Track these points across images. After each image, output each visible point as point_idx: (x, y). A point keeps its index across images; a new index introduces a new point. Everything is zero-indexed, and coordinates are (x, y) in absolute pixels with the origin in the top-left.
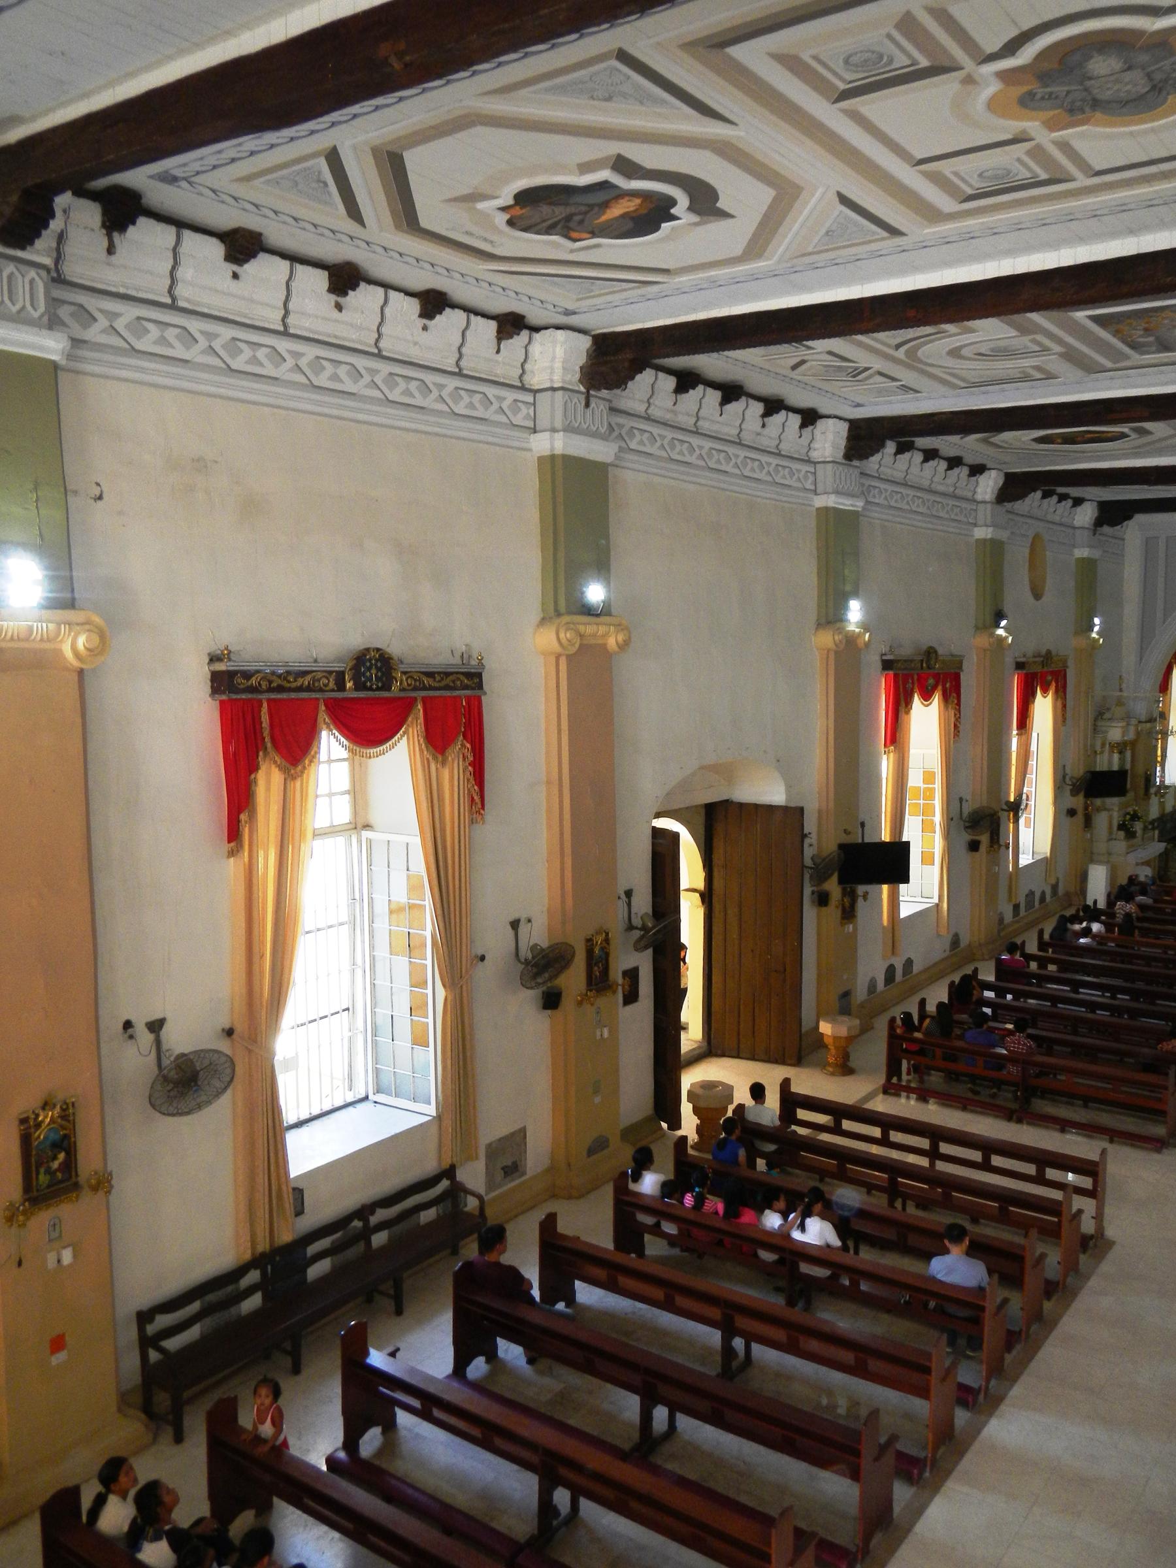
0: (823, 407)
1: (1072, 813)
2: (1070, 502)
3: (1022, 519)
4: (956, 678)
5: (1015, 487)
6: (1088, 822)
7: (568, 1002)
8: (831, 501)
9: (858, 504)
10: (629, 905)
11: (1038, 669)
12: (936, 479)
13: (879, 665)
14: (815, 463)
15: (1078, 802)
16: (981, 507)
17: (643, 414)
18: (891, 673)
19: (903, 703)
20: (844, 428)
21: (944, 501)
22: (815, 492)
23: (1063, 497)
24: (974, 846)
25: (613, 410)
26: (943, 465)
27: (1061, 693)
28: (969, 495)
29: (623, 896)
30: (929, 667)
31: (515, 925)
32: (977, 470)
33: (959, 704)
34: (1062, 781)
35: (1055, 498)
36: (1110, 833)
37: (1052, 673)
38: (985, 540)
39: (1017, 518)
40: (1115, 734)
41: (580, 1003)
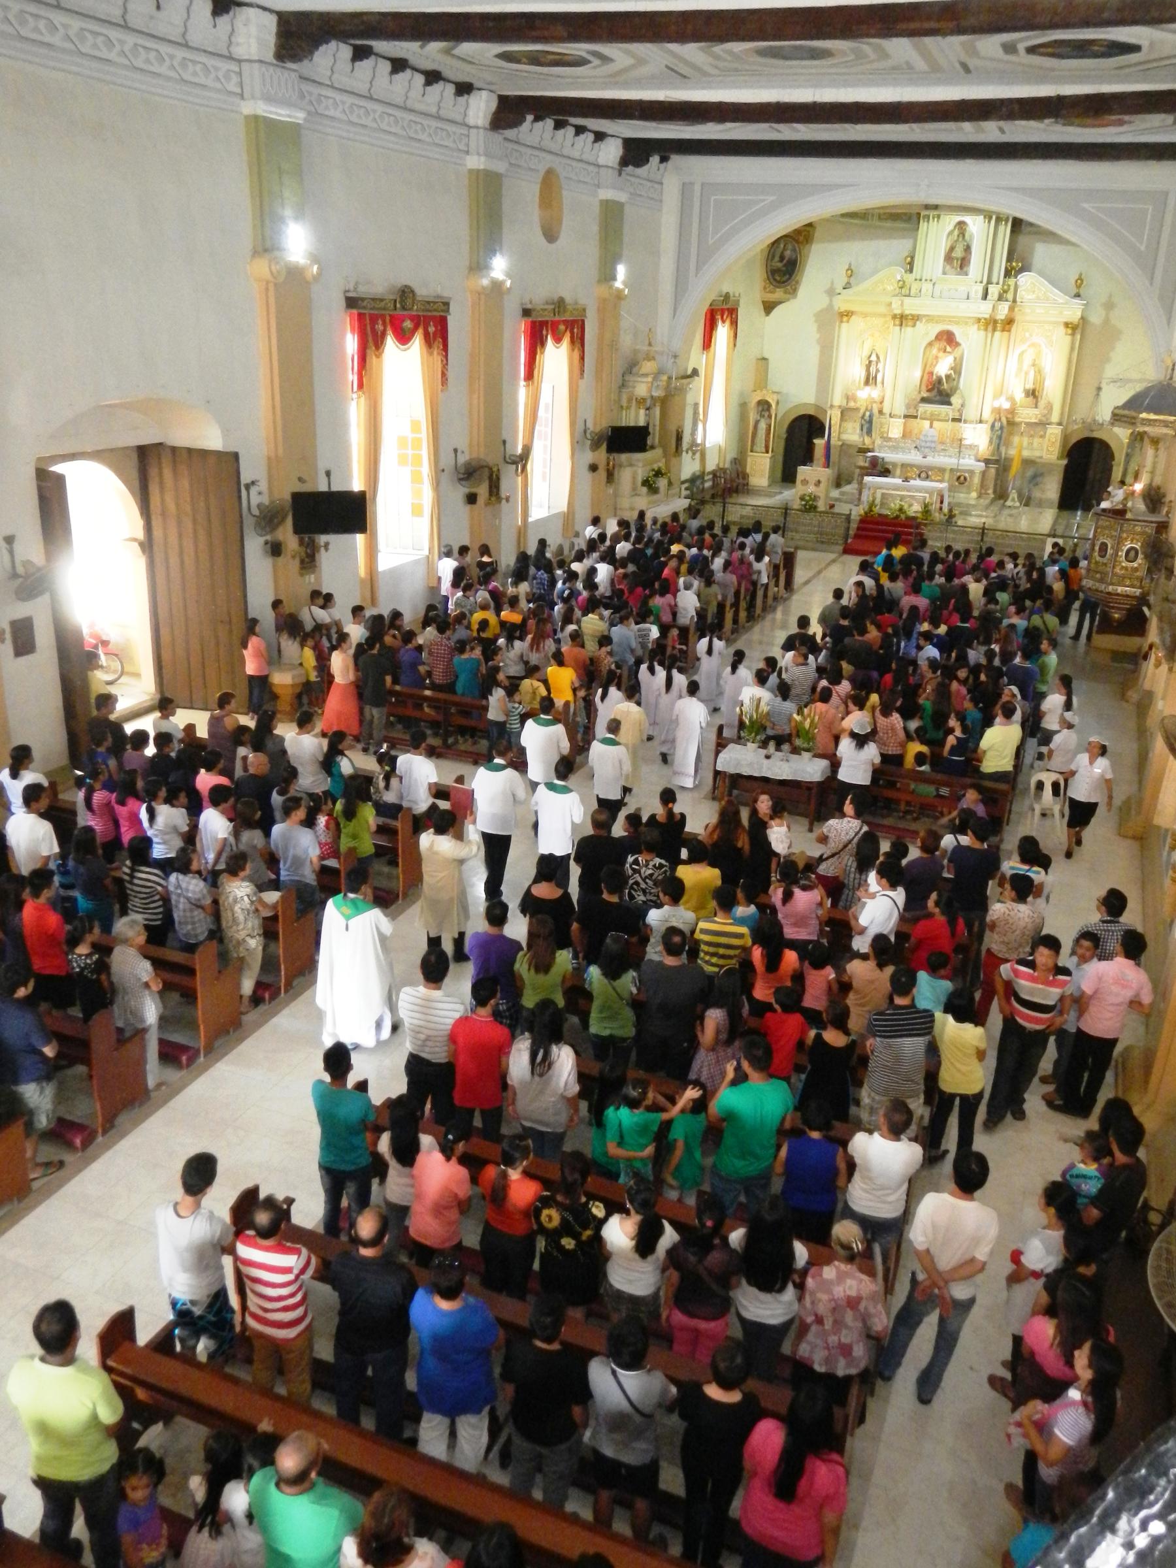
1: (593, 468)
2: (591, 137)
4: (442, 325)
5: (511, 111)
6: (610, 476)
9: (299, 116)
10: (11, 552)
12: (412, 94)
13: (343, 303)
14: (239, 61)
15: (601, 455)
18: (355, 311)
20: (271, 22)
21: (426, 122)
22: (242, 96)
23: (580, 130)
24: (471, 499)
26: (420, 79)
27: (578, 341)
28: (459, 118)
30: (404, 308)
32: (464, 89)
34: (583, 438)
35: (571, 131)
36: (634, 489)
37: (565, 322)
38: (478, 171)
39: (523, 149)
40: (642, 389)
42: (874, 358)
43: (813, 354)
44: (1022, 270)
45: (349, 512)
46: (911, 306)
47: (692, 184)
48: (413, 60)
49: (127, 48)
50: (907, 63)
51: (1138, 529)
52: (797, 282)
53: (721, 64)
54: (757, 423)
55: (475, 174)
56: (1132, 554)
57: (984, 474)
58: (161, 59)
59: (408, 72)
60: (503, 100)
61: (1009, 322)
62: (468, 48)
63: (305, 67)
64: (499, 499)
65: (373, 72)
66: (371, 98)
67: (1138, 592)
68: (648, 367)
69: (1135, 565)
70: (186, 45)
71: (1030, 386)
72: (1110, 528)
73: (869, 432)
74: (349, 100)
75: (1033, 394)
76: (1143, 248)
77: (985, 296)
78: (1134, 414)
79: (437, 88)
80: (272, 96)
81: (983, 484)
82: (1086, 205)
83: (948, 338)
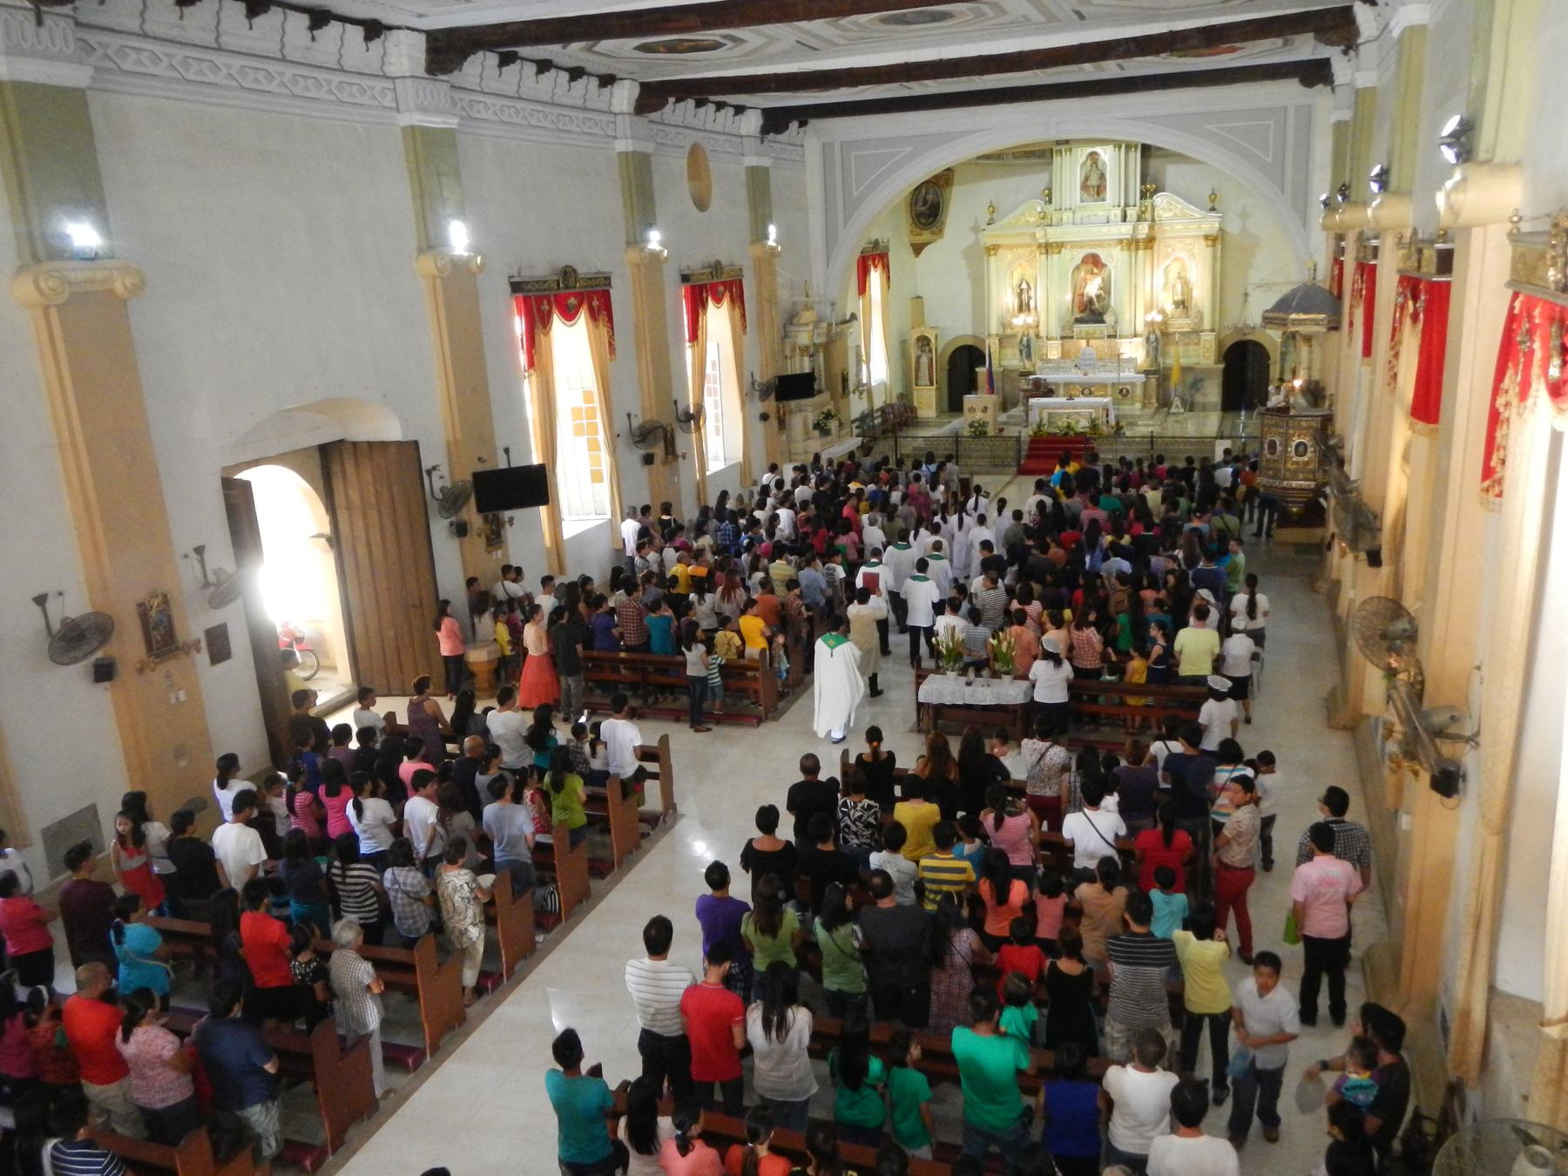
0: (387, 18)
1: (764, 417)
2: (731, 111)
3: (674, 130)
4: (605, 297)
5: (652, 97)
6: (782, 424)
7: (125, 673)
8: (417, 119)
9: (453, 122)
11: (706, 280)
12: (558, 91)
15: (771, 405)
16: (619, 118)
17: (137, 29)
18: (520, 295)
19: (538, 324)
20: (421, 41)
22: (398, 110)
23: (720, 106)
24: (648, 460)
25: (78, 24)
26: (565, 76)
27: (738, 300)
28: (604, 107)
29: (193, 555)
30: (567, 287)
31: (41, 600)
32: (607, 80)
33: (610, 320)
35: (711, 108)
36: (807, 433)
37: (724, 284)
39: (668, 129)
40: (804, 338)
41: (141, 671)
42: (1024, 286)
43: (965, 288)
44: (1156, 191)
45: (531, 486)
46: (1054, 235)
47: (832, 144)
48: (557, 60)
49: (286, 80)
50: (1024, 16)
51: (1304, 424)
52: (943, 223)
53: (848, 35)
54: (918, 358)
55: (625, 156)
56: (1301, 448)
57: (1145, 385)
58: (319, 85)
59: (553, 71)
60: (646, 88)
61: (1150, 241)
62: (606, 45)
63: (455, 77)
64: (676, 457)
65: (521, 76)
66: (520, 98)
67: (1312, 484)
68: (807, 316)
69: (1306, 459)
70: (342, 70)
71: (1178, 297)
72: (1276, 425)
73: (1029, 356)
74: (500, 102)
75: (1183, 304)
76: (1270, 160)
77: (1124, 219)
78: (1282, 315)
79: (582, 82)
80: (427, 107)
81: (1145, 395)
82: (1209, 127)
83: (1094, 261)
